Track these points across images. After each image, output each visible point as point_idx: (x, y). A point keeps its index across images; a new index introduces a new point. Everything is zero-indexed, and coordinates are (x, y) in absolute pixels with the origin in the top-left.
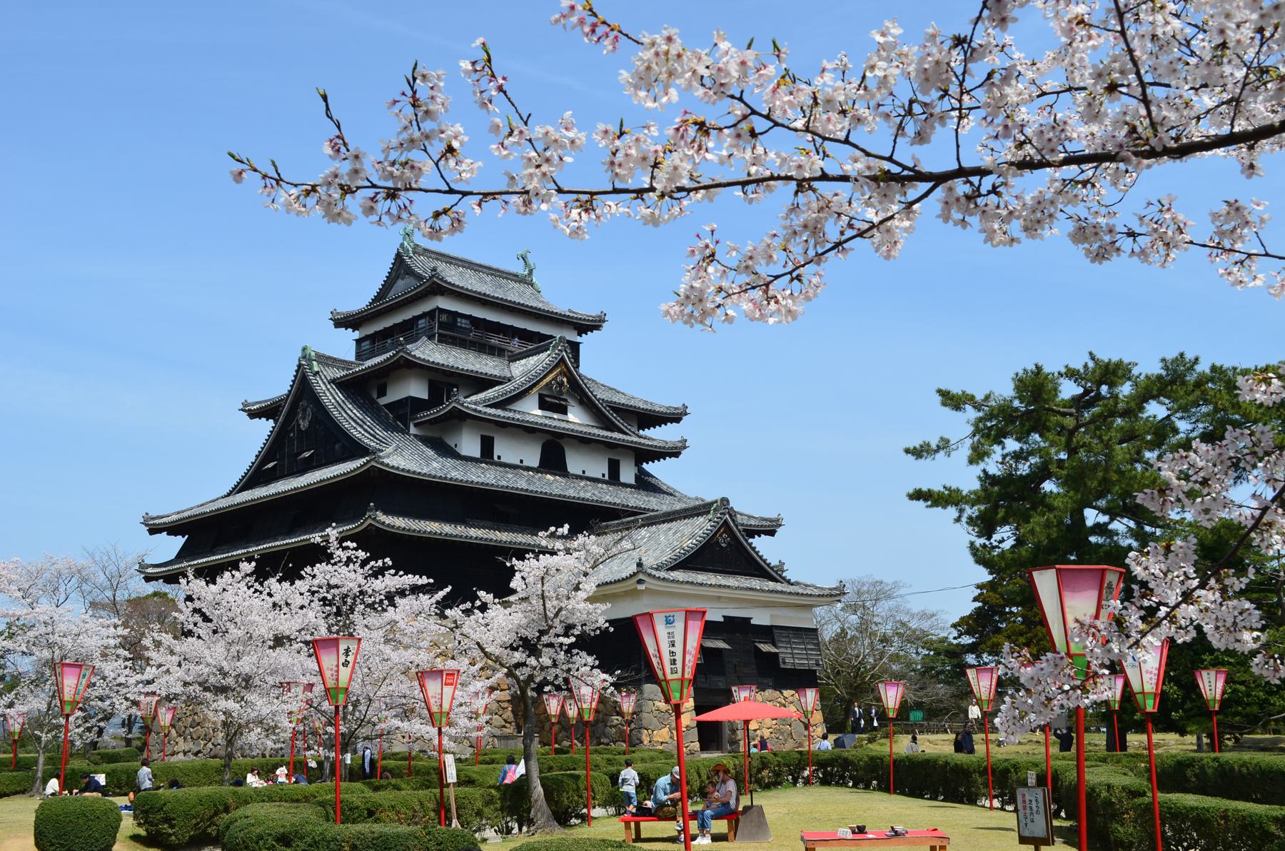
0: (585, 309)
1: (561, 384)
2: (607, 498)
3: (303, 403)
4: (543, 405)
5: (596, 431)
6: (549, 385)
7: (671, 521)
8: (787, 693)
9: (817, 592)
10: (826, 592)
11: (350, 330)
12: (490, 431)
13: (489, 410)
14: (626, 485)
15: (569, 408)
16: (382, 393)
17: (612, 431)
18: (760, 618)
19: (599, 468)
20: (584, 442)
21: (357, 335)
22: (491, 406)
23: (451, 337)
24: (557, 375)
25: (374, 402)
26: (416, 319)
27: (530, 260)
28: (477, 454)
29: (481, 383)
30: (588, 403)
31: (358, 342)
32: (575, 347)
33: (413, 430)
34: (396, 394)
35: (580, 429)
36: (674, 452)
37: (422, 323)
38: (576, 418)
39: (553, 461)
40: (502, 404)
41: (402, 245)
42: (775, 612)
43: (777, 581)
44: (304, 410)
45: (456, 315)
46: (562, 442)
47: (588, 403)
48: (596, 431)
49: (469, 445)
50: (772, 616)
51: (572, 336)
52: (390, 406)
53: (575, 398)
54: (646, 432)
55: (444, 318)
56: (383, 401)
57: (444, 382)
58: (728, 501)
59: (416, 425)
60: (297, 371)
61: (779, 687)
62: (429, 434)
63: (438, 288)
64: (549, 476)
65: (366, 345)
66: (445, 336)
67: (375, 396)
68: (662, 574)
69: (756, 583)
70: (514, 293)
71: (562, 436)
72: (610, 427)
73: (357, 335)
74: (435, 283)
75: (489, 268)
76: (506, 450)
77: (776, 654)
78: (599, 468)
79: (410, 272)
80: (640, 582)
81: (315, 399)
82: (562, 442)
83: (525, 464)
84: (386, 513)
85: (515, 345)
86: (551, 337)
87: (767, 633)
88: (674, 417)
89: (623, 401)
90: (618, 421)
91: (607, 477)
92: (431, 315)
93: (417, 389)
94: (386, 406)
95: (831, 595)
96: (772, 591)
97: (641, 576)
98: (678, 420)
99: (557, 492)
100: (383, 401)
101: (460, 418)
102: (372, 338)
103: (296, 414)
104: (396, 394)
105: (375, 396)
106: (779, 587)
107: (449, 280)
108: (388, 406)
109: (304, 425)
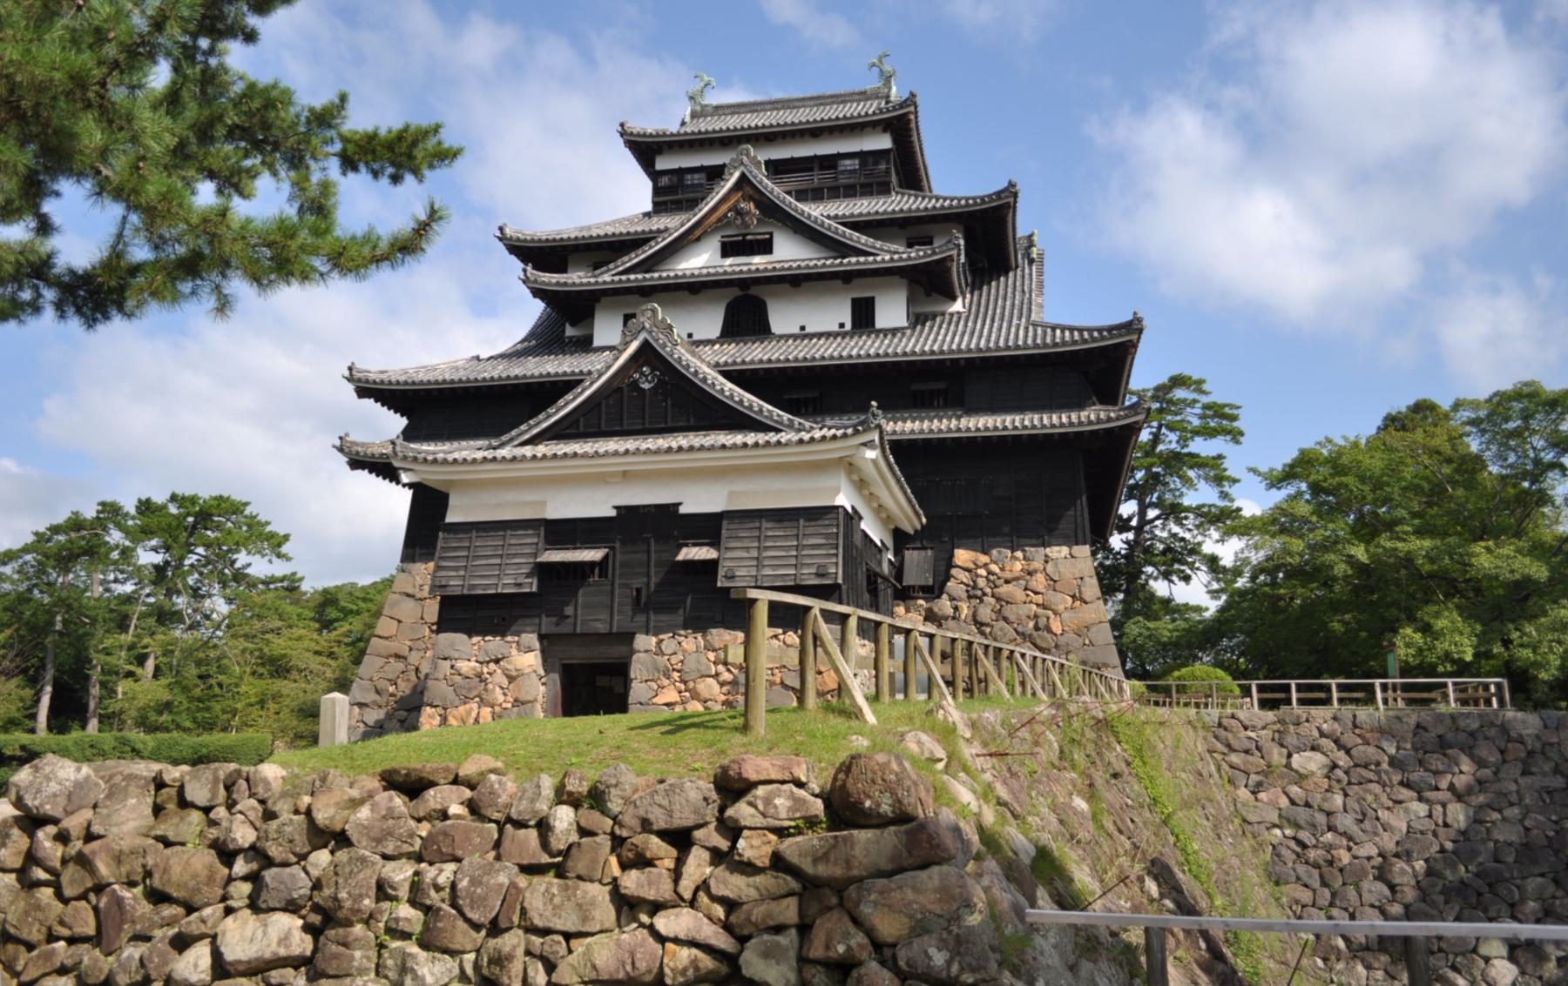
4: (728, 250)
13: (624, 278)
18: (698, 500)
19: (834, 314)
20: (796, 282)
23: (673, 202)
40: (648, 265)
42: (741, 486)
46: (754, 291)
50: (731, 494)
66: (664, 203)
75: (818, 98)
77: (712, 565)
82: (754, 291)
90: (862, 240)
91: (848, 327)
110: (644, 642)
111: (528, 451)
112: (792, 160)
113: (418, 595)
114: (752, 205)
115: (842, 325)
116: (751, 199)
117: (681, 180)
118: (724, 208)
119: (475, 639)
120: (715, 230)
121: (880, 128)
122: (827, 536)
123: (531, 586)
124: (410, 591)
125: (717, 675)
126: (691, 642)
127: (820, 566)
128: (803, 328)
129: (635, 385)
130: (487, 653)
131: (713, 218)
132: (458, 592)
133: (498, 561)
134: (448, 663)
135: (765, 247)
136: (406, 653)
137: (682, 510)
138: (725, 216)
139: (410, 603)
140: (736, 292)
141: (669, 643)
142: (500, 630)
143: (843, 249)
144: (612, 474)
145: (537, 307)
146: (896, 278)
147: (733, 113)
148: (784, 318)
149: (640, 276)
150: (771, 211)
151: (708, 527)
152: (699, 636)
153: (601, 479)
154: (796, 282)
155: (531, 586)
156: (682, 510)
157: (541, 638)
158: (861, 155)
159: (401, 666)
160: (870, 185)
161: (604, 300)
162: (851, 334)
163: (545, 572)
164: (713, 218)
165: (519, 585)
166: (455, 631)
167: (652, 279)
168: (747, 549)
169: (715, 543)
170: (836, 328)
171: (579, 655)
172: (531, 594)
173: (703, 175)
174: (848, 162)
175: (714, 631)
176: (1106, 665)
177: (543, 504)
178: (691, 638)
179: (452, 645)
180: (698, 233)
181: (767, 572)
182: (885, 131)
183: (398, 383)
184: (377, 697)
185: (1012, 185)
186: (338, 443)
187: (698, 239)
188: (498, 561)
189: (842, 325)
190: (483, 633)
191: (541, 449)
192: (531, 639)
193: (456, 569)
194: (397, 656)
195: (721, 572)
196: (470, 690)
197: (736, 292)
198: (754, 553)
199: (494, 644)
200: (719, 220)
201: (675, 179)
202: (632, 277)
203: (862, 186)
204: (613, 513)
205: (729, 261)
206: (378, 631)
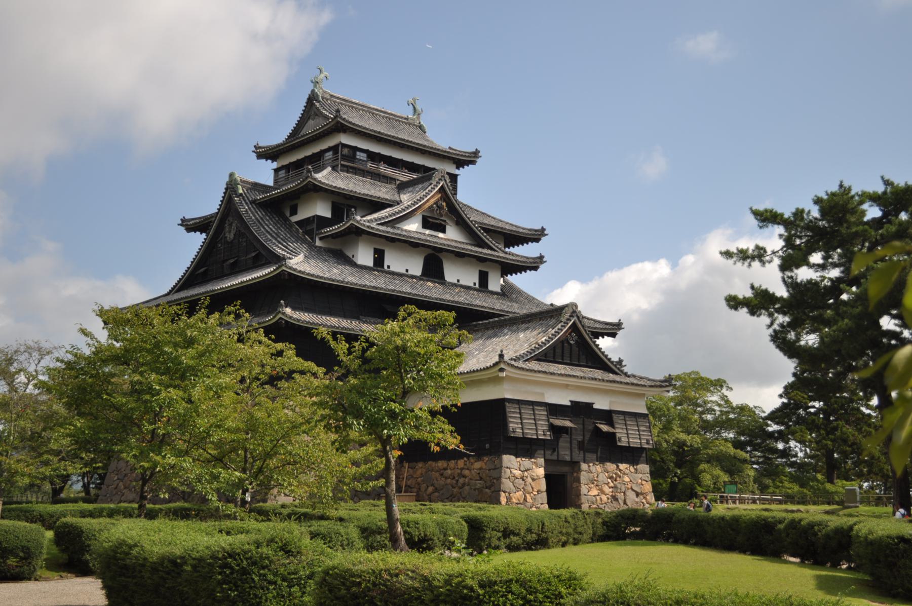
0: (464, 146)
1: (440, 208)
2: (478, 302)
3: (230, 219)
4: (426, 224)
5: (469, 247)
6: (431, 207)
7: (529, 321)
8: (623, 466)
9: (649, 383)
10: (658, 383)
11: (269, 161)
12: (383, 244)
13: (381, 228)
14: (493, 293)
15: (448, 228)
16: (294, 212)
17: (483, 248)
18: (601, 403)
19: (470, 278)
20: (459, 256)
21: (275, 165)
22: (382, 224)
23: (351, 168)
24: (438, 200)
25: (286, 220)
26: (323, 152)
27: (418, 107)
28: (370, 262)
29: (376, 205)
30: (462, 223)
31: (276, 171)
32: (454, 178)
33: (318, 243)
34: (304, 213)
35: (454, 244)
36: (534, 265)
37: (329, 155)
38: (452, 235)
39: (433, 270)
40: (393, 223)
41: (313, 91)
43: (616, 374)
44: (231, 225)
45: (355, 149)
46: (440, 255)
47: (462, 223)
48: (469, 247)
49: (364, 257)
50: (611, 403)
51: (452, 169)
52: (301, 223)
53: (451, 219)
54: (512, 250)
55: (346, 151)
56: (294, 219)
57: (344, 204)
58: (576, 306)
59: (321, 239)
60: (225, 193)
61: (617, 460)
62: (332, 247)
63: (341, 127)
64: (429, 284)
65: (282, 173)
67: (288, 214)
68: (520, 364)
69: (598, 374)
70: (404, 134)
71: (441, 250)
72: (481, 244)
73: (275, 165)
74: (338, 122)
76: (395, 262)
78: (470, 278)
79: (318, 114)
80: (502, 370)
81: (239, 216)
82: (440, 255)
83: (410, 273)
84: (294, 308)
85: (404, 176)
86: (434, 169)
87: (608, 416)
88: (536, 236)
89: (493, 223)
91: (477, 286)
92: (334, 149)
93: (322, 210)
94: (297, 223)
95: (661, 386)
96: (611, 382)
97: (502, 366)
98: (537, 240)
99: (435, 296)
100: (294, 219)
101: (357, 233)
102: (287, 168)
103: (223, 228)
104: (304, 213)
105: (288, 214)
106: (617, 378)
107: (351, 120)
108: (298, 223)
109: (230, 236)
114: (444, 204)
116: (444, 201)
117: (355, 155)
118: (432, 201)
119: (519, 459)
122: (646, 426)
134: (508, 470)
137: (595, 406)
138: (432, 206)
140: (430, 251)
141: (593, 468)
144: (572, 386)
145: (787, 368)
153: (567, 386)
154: (459, 256)
157: (546, 461)
166: (510, 454)
169: (611, 424)
170: (472, 285)
173: (365, 155)
175: (608, 464)
177: (543, 394)
179: (510, 461)
181: (631, 440)
182: (454, 163)
185: (543, 229)
189: (475, 284)
192: (541, 461)
193: (517, 423)
204: (569, 404)
205: (427, 232)
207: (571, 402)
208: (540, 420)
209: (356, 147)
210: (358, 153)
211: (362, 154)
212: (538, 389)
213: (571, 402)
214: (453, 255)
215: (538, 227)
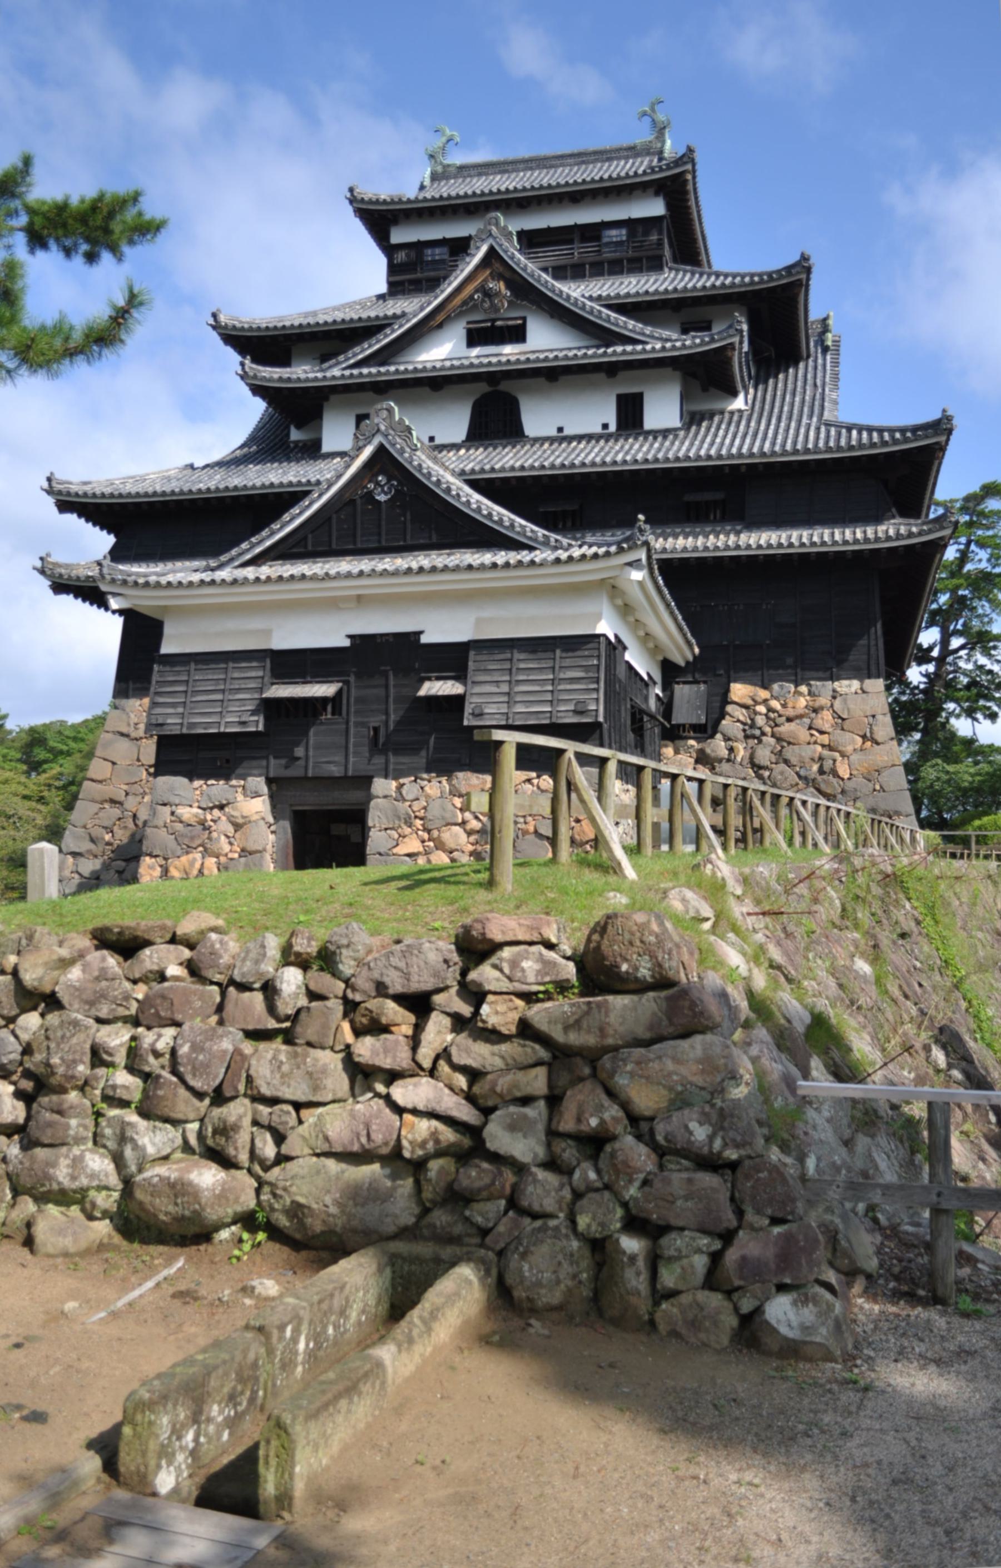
4: (474, 338)
13: (355, 372)
18: (441, 628)
20: (552, 375)
23: (411, 282)
42: (489, 612)
46: (504, 386)
50: (479, 622)
66: (401, 283)
75: (579, 155)
82: (504, 386)
90: (629, 325)
91: (613, 428)
110: (382, 786)
111: (250, 573)
112: (549, 229)
113: (133, 735)
114: (502, 285)
115: (605, 426)
116: (500, 277)
117: (420, 255)
119: (197, 783)
120: (460, 314)
121: (651, 191)
122: (586, 668)
123: (257, 724)
124: (124, 730)
125: (464, 823)
126: (435, 787)
127: (579, 702)
128: (560, 430)
129: (369, 496)
130: (210, 799)
131: (458, 300)
132: (176, 731)
133: (219, 697)
134: (167, 810)
135: (517, 334)
136: (121, 797)
137: (424, 639)
139: (124, 744)
140: (484, 388)
141: (410, 787)
142: (224, 771)
143: (606, 336)
145: (258, 407)
146: (669, 371)
147: (480, 175)
148: (539, 418)
149: (374, 370)
150: (524, 291)
151: (453, 659)
152: (444, 780)
153: (332, 605)
155: (257, 724)
156: (424, 639)
157: (269, 781)
158: (629, 224)
159: (116, 812)
160: (639, 260)
161: (333, 398)
162: (616, 437)
163: (271, 708)
164: (458, 300)
165: (243, 723)
167: (388, 373)
168: (497, 683)
169: (461, 676)
170: (598, 429)
171: (311, 801)
172: (256, 734)
174: (614, 232)
175: (460, 775)
176: (898, 813)
177: (268, 633)
178: (434, 782)
179: (171, 789)
180: (440, 318)
181: (520, 708)
182: (657, 194)
183: (103, 495)
184: (92, 846)
185: (804, 258)
186: (39, 564)
187: (440, 326)
188: (219, 697)
189: (605, 426)
190: (206, 776)
191: (265, 571)
192: (258, 783)
193: (174, 705)
194: (113, 802)
195: (468, 709)
196: (192, 838)
197: (484, 388)
198: (505, 688)
199: (218, 788)
200: (465, 303)
201: (413, 254)
202: (365, 371)
203: (630, 260)
204: (346, 643)
205: (476, 351)
206: (91, 774)
207: (349, 636)
208: (239, 690)
209: (419, 242)
210: (429, 251)
211: (437, 251)
212: (256, 623)
213: (349, 636)
214: (542, 380)
215: (793, 258)
